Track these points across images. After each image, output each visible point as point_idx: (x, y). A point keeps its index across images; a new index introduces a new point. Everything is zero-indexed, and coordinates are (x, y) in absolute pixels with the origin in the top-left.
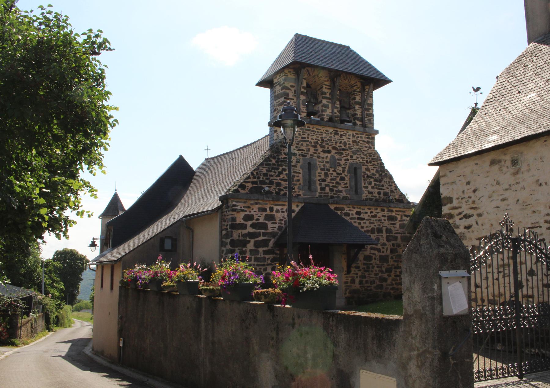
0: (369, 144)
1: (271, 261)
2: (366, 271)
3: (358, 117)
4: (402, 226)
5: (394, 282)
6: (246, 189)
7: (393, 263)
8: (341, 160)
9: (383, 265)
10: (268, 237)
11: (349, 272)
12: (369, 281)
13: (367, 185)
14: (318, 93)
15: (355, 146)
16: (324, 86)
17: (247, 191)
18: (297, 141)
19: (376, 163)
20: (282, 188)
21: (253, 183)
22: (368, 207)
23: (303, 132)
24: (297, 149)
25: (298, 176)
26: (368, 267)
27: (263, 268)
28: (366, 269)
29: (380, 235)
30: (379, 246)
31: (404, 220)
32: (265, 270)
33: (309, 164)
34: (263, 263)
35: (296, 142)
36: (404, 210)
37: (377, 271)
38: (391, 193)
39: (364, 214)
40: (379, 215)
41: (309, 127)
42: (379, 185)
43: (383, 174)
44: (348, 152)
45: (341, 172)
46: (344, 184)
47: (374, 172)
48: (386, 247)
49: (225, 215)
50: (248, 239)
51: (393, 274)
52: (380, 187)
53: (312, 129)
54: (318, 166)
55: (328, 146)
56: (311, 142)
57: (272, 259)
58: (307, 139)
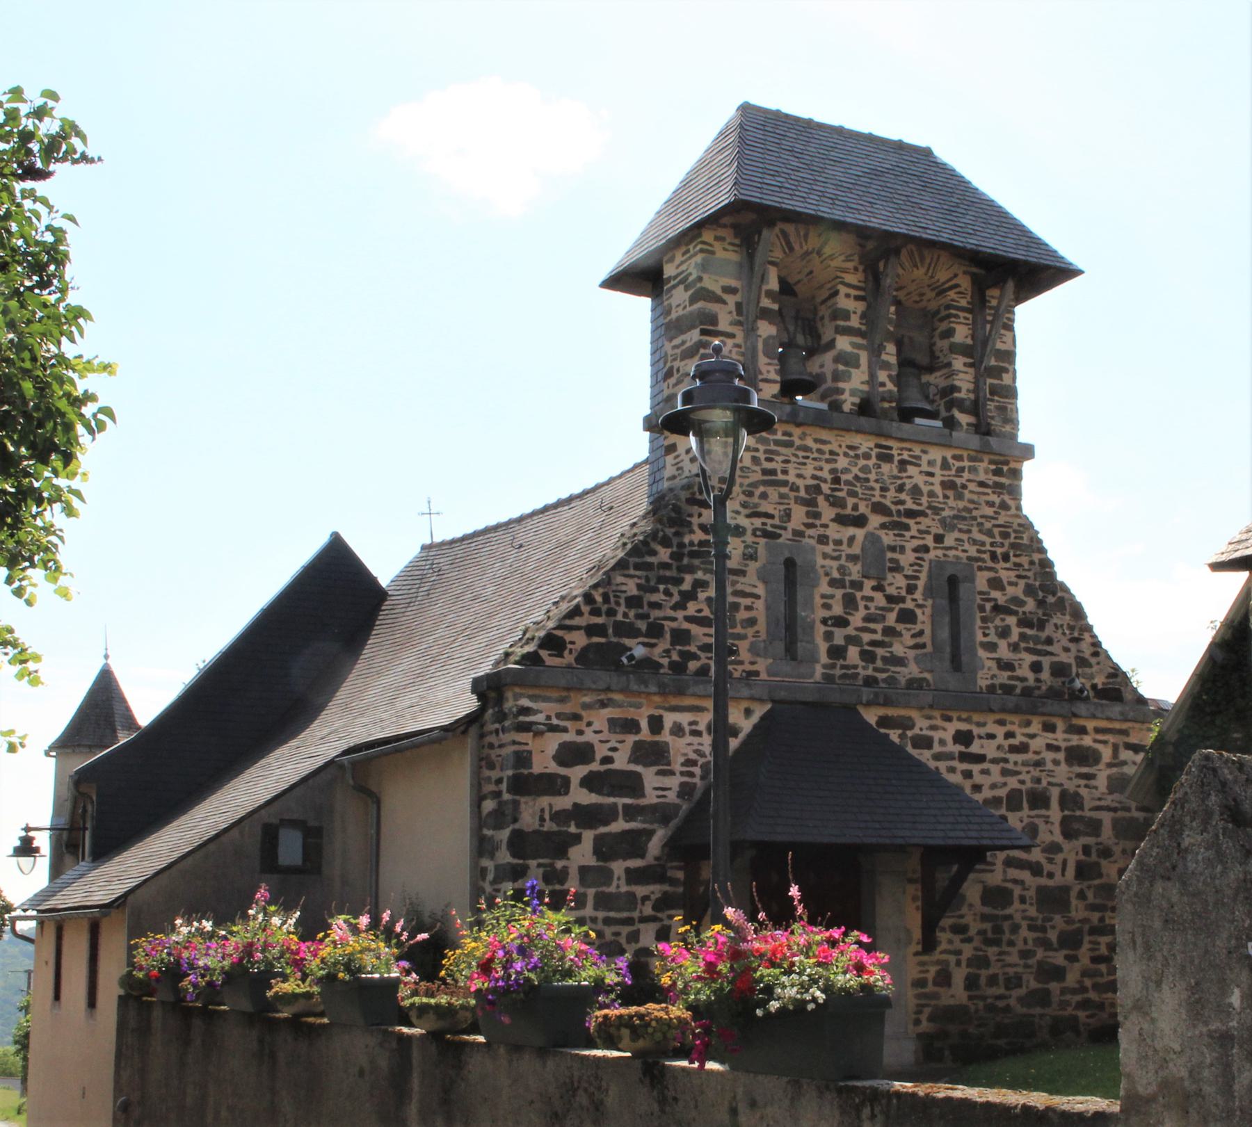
0: (999, 494)
1: (654, 908)
2: (989, 942)
3: (963, 400)
4: (1117, 784)
5: (1088, 982)
6: (566, 653)
7: (1086, 914)
8: (902, 549)
9: (1051, 920)
10: (643, 822)
11: (929, 944)
12: (1001, 979)
13: (993, 638)
14: (820, 314)
15: (951, 502)
16: (843, 290)
17: (569, 658)
18: (747, 482)
19: (1024, 560)
20: (693, 649)
21: (591, 630)
22: (998, 716)
23: (766, 452)
24: (747, 511)
25: (749, 608)
26: (998, 930)
27: (625, 930)
28: (990, 935)
29: (1038, 816)
30: (1036, 855)
31: (1124, 763)
32: (634, 937)
33: (790, 564)
34: (625, 915)
35: (741, 485)
36: (1124, 726)
37: (1030, 942)
38: (1078, 666)
39: (985, 741)
40: (1037, 744)
41: (790, 435)
42: (1036, 640)
43: (1051, 599)
44: (925, 522)
45: (903, 593)
46: (913, 636)
47: (1018, 591)
48: (1059, 858)
49: (491, 746)
50: (573, 829)
51: (1084, 953)
52: (1039, 647)
53: (798, 442)
54: (821, 571)
55: (854, 500)
56: (795, 488)
57: (657, 900)
58: (781, 477)
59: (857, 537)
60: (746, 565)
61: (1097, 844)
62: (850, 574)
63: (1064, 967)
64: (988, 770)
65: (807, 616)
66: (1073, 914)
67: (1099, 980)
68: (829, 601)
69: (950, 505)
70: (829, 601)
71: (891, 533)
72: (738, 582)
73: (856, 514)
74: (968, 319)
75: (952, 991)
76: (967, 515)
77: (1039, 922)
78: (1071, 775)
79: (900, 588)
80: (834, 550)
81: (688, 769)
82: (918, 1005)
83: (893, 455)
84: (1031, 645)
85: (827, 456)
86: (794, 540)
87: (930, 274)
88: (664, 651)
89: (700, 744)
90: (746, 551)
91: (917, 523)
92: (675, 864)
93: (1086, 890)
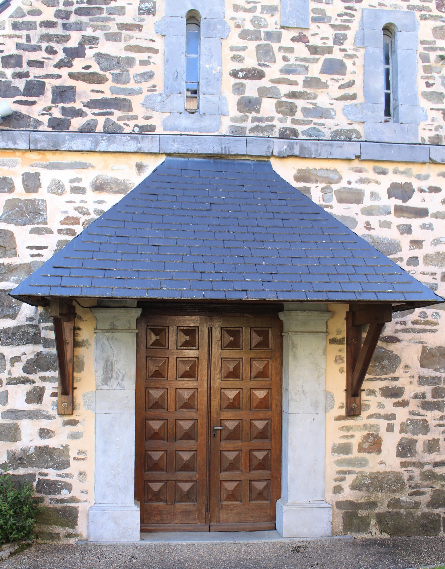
1: (25, 370)
2: (426, 406)
20: (78, 105)
25: (144, 63)
28: (429, 398)
39: (426, 195)
45: (330, 43)
54: (232, 24)
60: (143, 20)
62: (266, 26)
64: (431, 225)
65: (211, 68)
72: (133, 37)
75: (382, 456)
79: (327, 38)
82: (339, 472)
88: (44, 109)
90: (143, 6)
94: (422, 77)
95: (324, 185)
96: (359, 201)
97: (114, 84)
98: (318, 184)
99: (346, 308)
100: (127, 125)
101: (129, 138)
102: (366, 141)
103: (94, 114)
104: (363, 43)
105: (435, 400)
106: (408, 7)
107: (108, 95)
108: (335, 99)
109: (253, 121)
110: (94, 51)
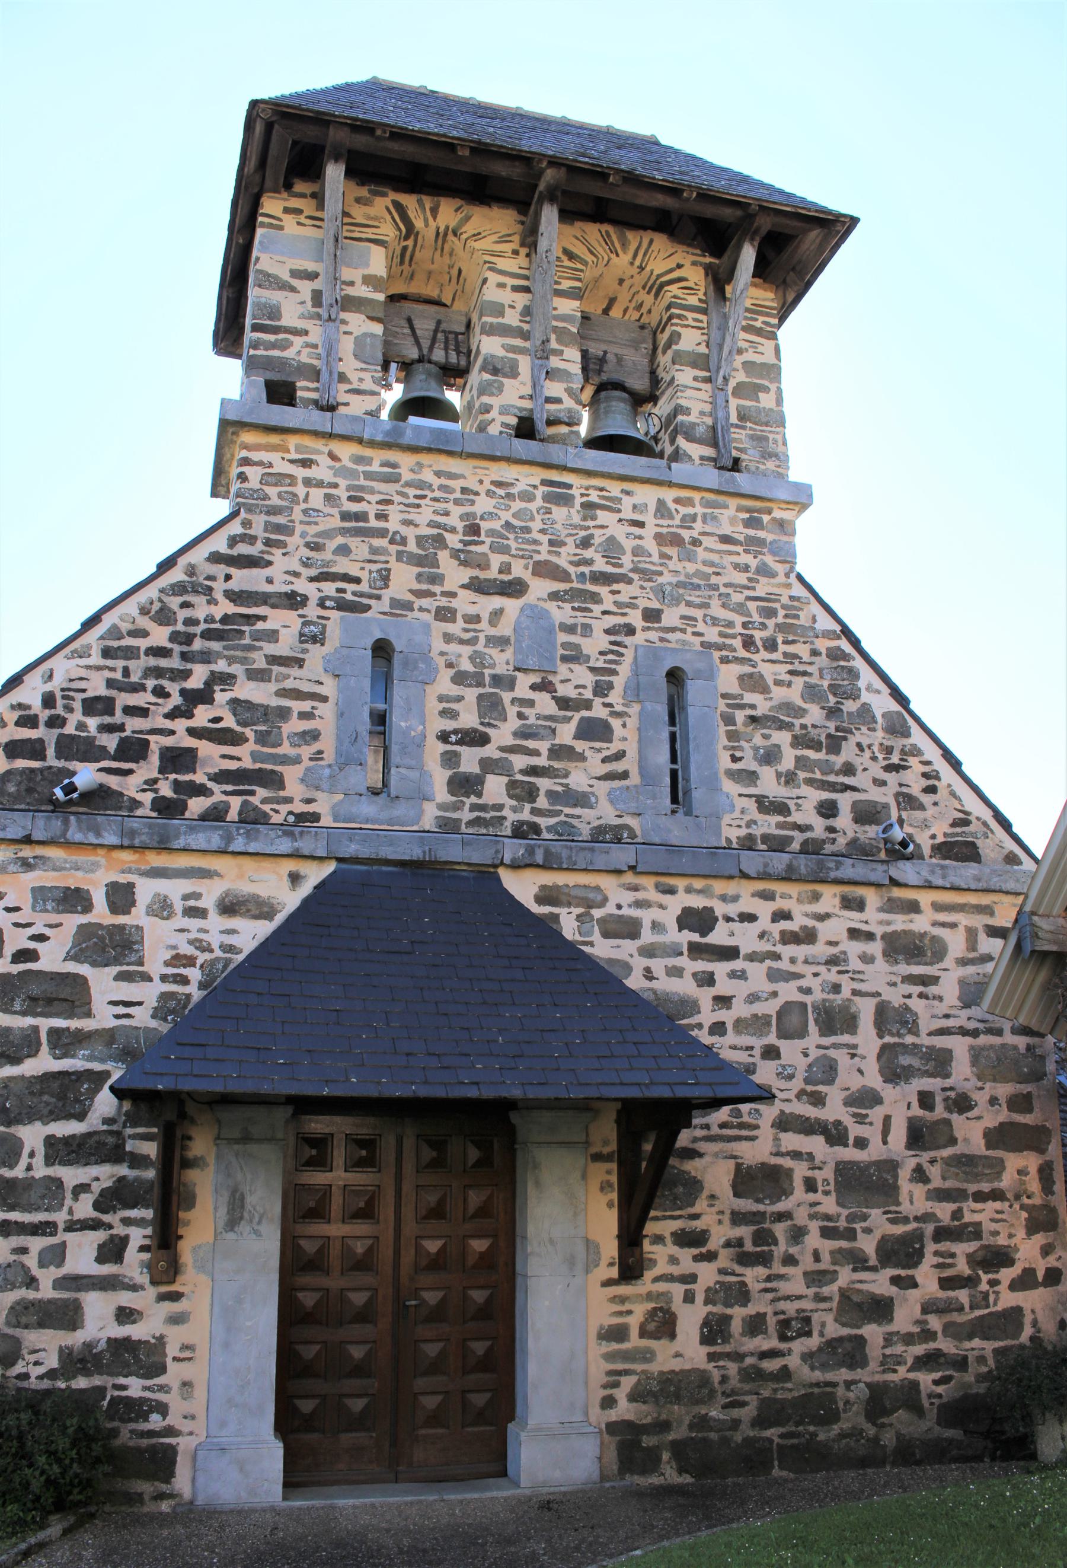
1: (97, 1206)
2: (745, 1259)
3: (694, 425)
5: (935, 1323)
7: (928, 1206)
8: (587, 630)
9: (865, 1218)
10: (90, 1058)
12: (771, 1321)
13: (749, 763)
16: (493, 278)
18: (312, 530)
19: (802, 650)
20: (199, 778)
22: (761, 886)
23: (349, 488)
24: (313, 572)
25: (304, 716)
26: (763, 1237)
27: (37, 1244)
28: (749, 1247)
29: (835, 1046)
30: (834, 1110)
32: (56, 1255)
33: (382, 650)
36: (985, 900)
37: (826, 1257)
39: (736, 926)
40: (826, 930)
43: (850, 706)
44: (626, 592)
45: (588, 694)
47: (794, 694)
48: (876, 1114)
51: (926, 1275)
52: (832, 778)
53: (406, 476)
54: (441, 661)
55: (506, 558)
57: (103, 1193)
58: (373, 523)
59: (507, 611)
60: (305, 651)
61: (944, 1089)
62: (493, 666)
63: (892, 1299)
64: (743, 972)
65: (409, 728)
66: (905, 1208)
67: (957, 1318)
68: (454, 706)
69: (671, 567)
70: (454, 706)
71: (567, 606)
72: (289, 677)
73: (506, 578)
74: (701, 321)
75: (677, 1345)
76: (702, 583)
77: (842, 1223)
78: (894, 979)
79: (584, 687)
80: (467, 630)
81: (175, 971)
82: (610, 1373)
83: (573, 497)
84: (818, 775)
85: (458, 495)
86: (392, 614)
87: (637, 263)
88: (146, 782)
89: (200, 930)
90: (306, 630)
91: (614, 592)
92: (140, 1130)
93: (926, 1166)
94: (725, 748)
95: (580, 910)
96: (634, 935)
97: (258, 748)
98: (572, 909)
99: (619, 1105)
100: (277, 812)
101: (280, 833)
102: (644, 844)
103: (225, 793)
104: (638, 695)
105: (758, 1249)
106: (702, 644)
107: (247, 764)
108: (596, 778)
109: (471, 810)
110: (228, 695)
